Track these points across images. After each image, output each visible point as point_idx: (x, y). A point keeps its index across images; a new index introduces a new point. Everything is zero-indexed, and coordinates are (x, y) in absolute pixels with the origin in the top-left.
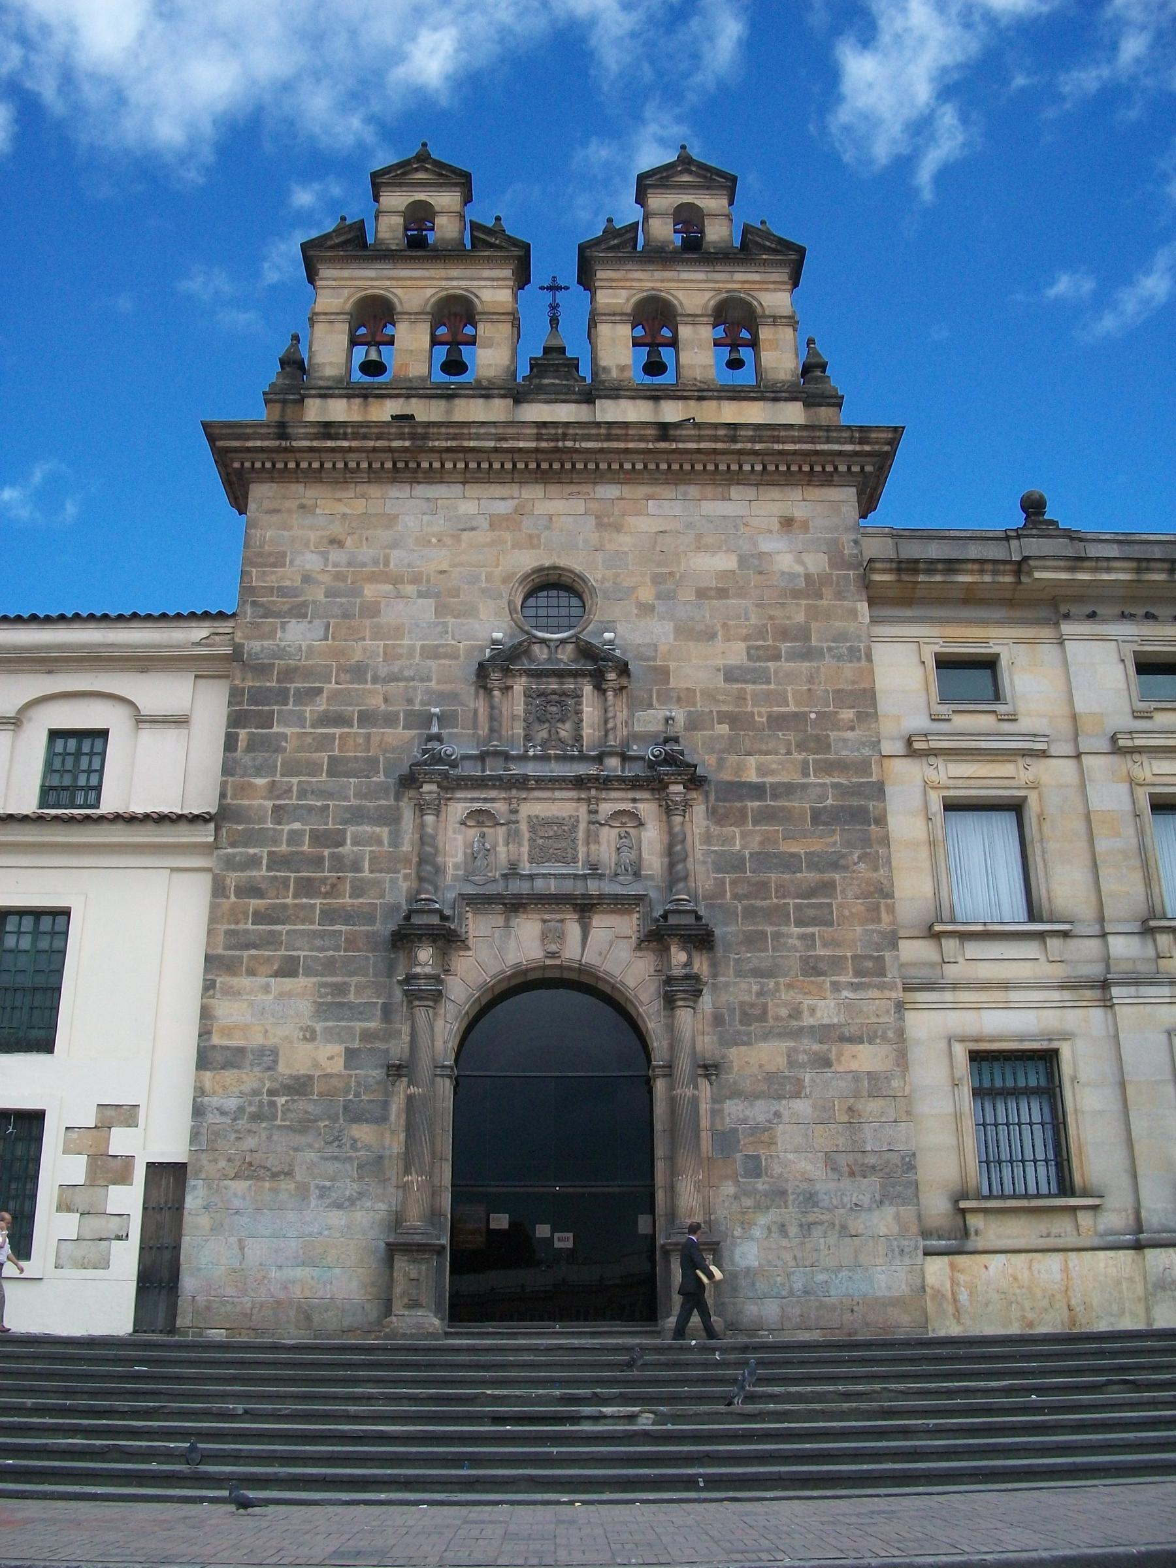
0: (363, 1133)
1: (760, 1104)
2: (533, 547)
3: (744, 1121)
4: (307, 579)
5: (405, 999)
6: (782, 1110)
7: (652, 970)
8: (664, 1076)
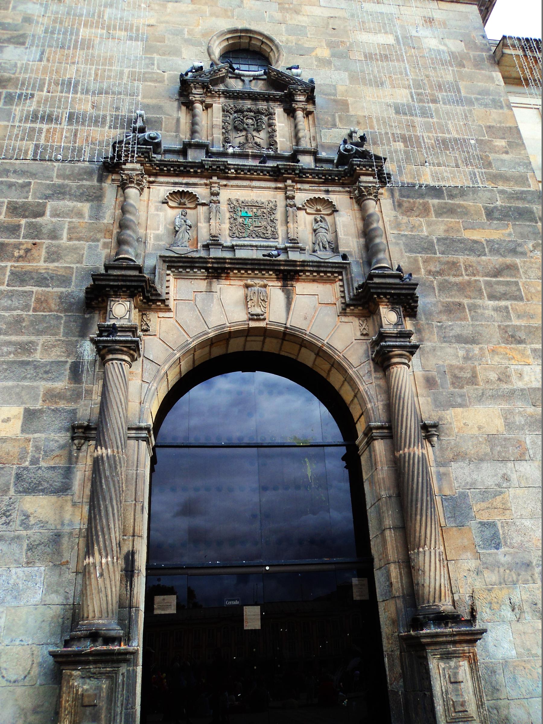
1: (485, 465)
2: (229, 17)
3: (473, 485)
4: (27, 20)
5: (98, 358)
6: (509, 473)
7: (359, 334)
8: (383, 438)
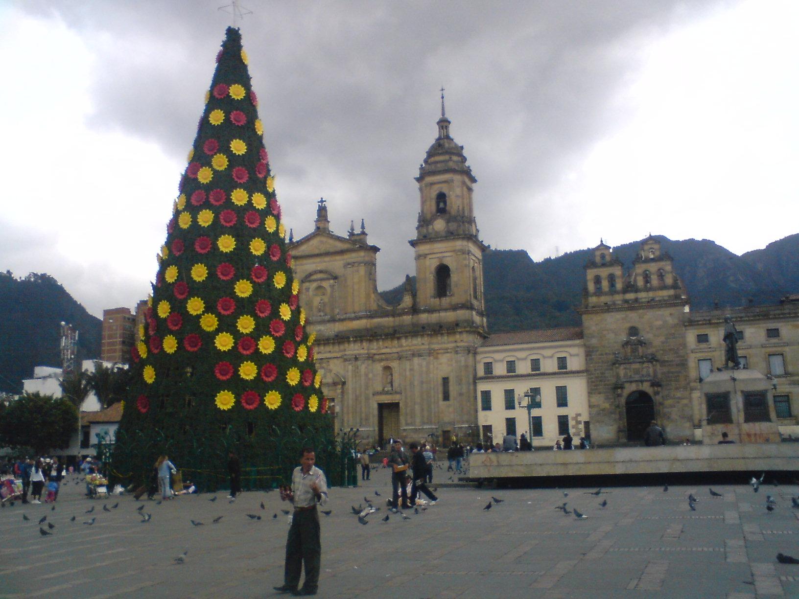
0: (613, 415)
